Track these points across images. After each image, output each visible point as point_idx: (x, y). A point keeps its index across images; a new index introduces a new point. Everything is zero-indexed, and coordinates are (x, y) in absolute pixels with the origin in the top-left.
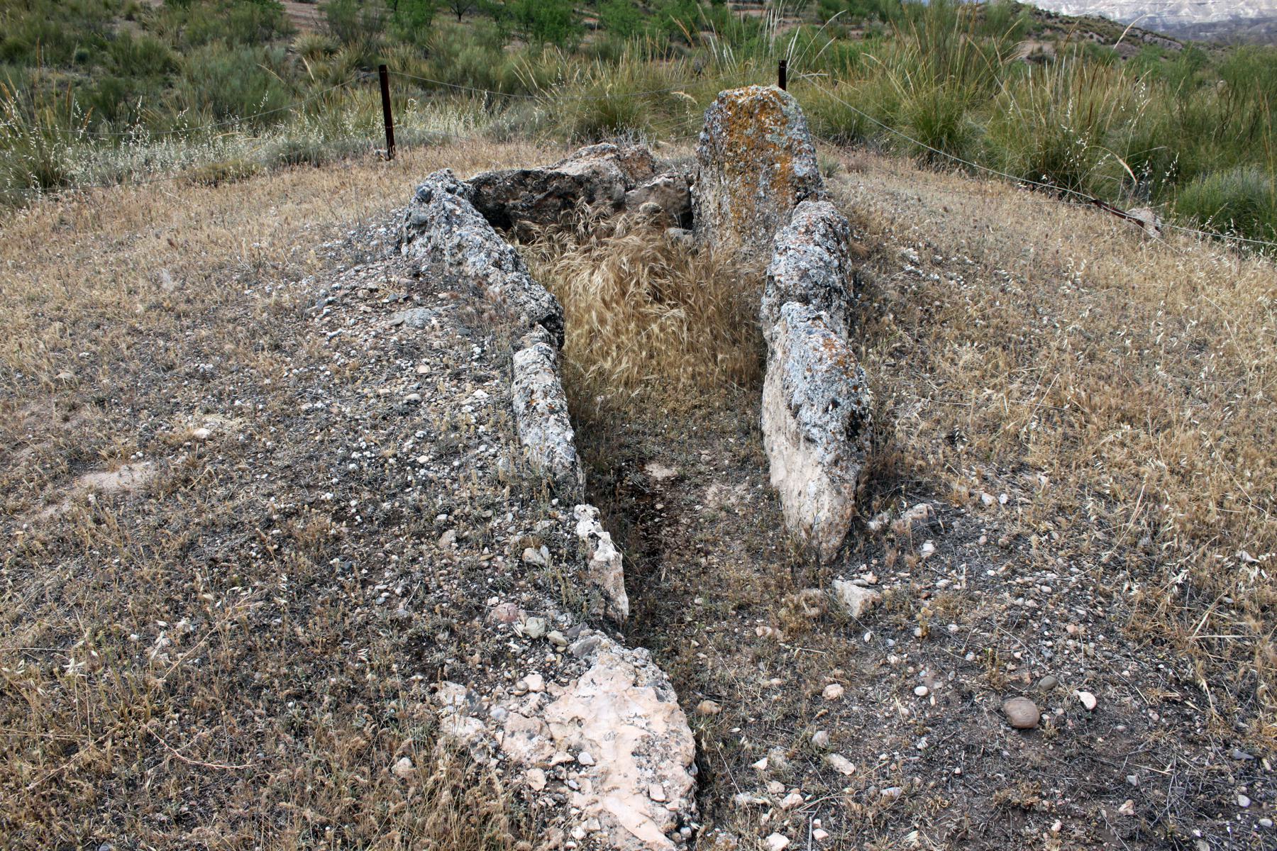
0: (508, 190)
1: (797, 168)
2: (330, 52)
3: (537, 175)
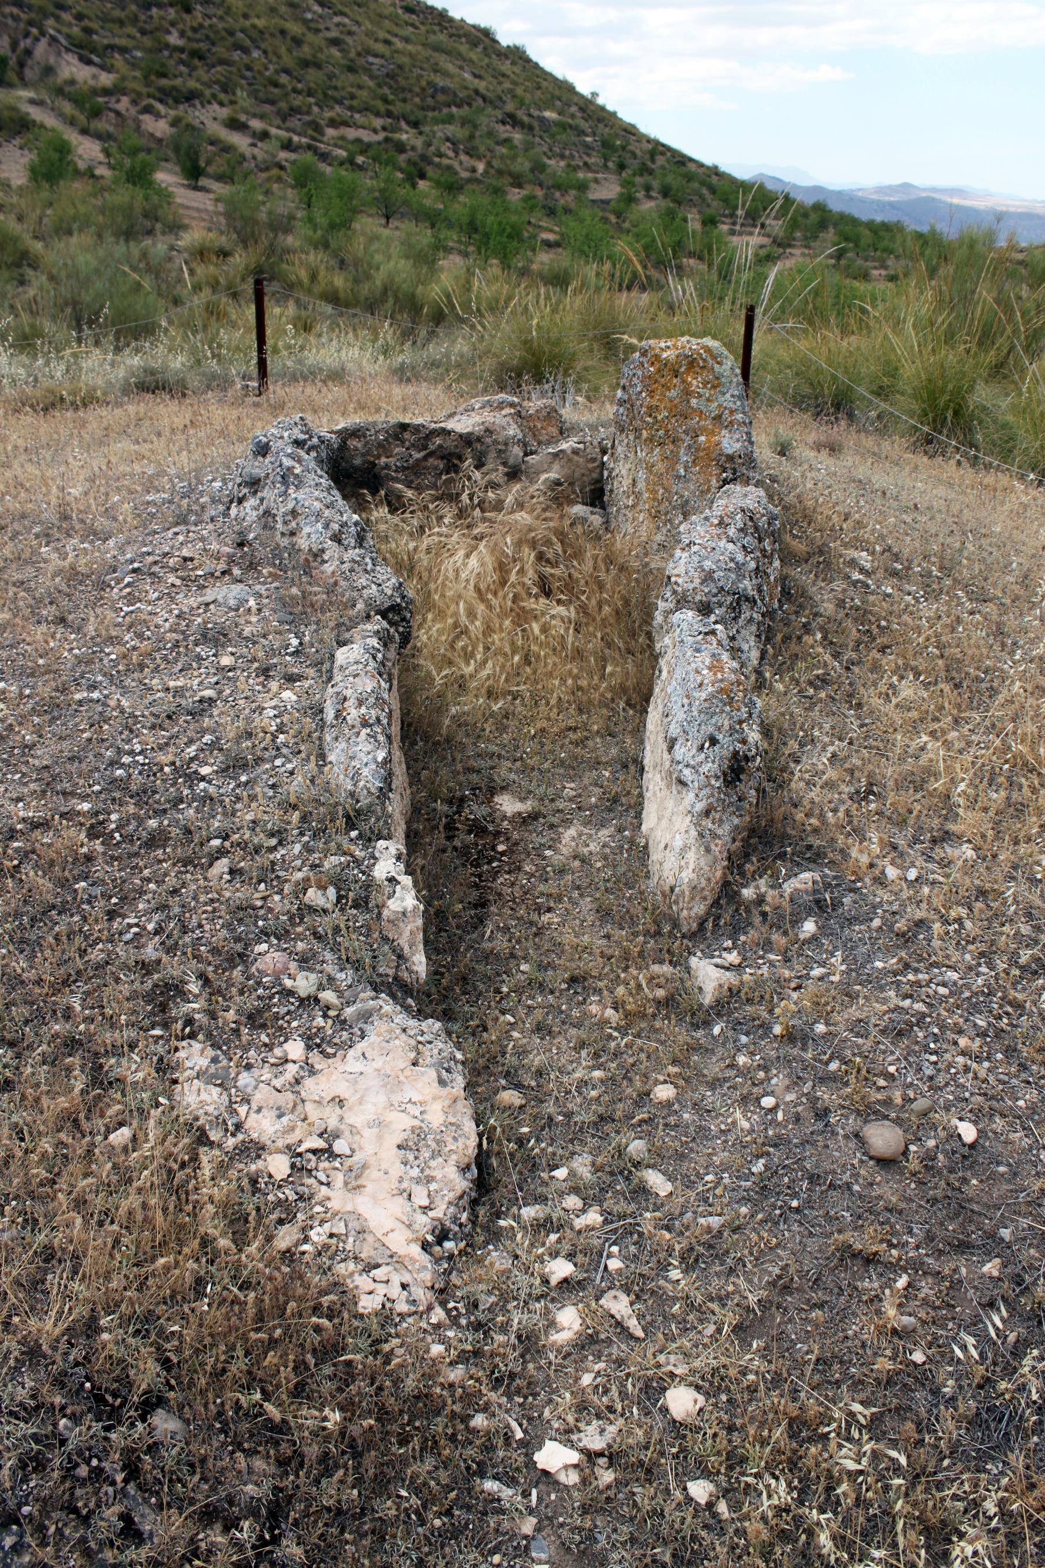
0: (380, 445)
1: (725, 443)
2: (224, 254)
3: (417, 429)
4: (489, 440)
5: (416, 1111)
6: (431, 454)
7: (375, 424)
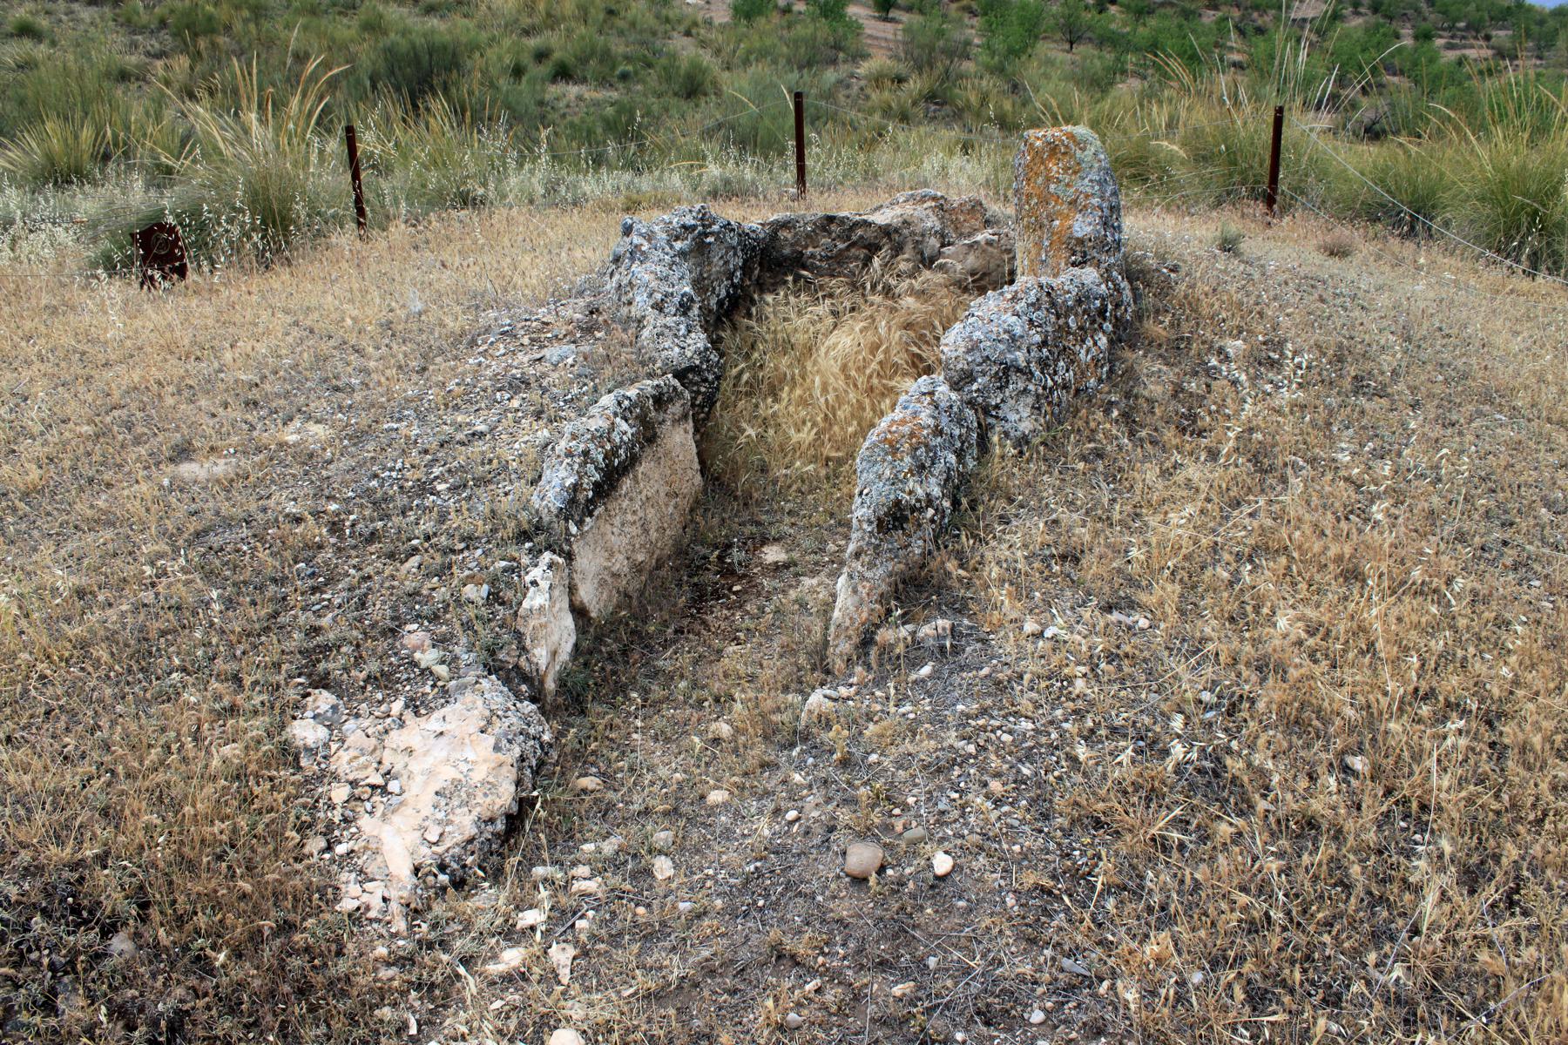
0: (808, 236)
1: (1076, 227)
2: (900, 80)
3: (842, 221)
4: (906, 232)
5: (464, 767)
6: (853, 244)
7: (804, 217)
